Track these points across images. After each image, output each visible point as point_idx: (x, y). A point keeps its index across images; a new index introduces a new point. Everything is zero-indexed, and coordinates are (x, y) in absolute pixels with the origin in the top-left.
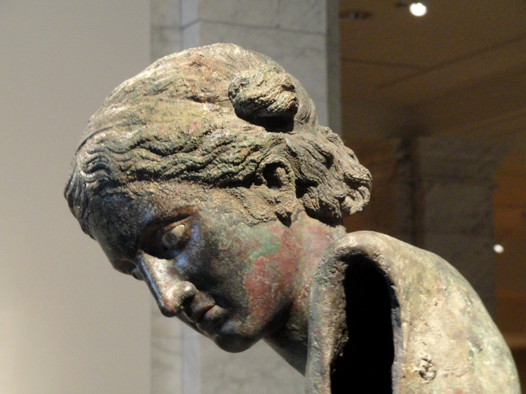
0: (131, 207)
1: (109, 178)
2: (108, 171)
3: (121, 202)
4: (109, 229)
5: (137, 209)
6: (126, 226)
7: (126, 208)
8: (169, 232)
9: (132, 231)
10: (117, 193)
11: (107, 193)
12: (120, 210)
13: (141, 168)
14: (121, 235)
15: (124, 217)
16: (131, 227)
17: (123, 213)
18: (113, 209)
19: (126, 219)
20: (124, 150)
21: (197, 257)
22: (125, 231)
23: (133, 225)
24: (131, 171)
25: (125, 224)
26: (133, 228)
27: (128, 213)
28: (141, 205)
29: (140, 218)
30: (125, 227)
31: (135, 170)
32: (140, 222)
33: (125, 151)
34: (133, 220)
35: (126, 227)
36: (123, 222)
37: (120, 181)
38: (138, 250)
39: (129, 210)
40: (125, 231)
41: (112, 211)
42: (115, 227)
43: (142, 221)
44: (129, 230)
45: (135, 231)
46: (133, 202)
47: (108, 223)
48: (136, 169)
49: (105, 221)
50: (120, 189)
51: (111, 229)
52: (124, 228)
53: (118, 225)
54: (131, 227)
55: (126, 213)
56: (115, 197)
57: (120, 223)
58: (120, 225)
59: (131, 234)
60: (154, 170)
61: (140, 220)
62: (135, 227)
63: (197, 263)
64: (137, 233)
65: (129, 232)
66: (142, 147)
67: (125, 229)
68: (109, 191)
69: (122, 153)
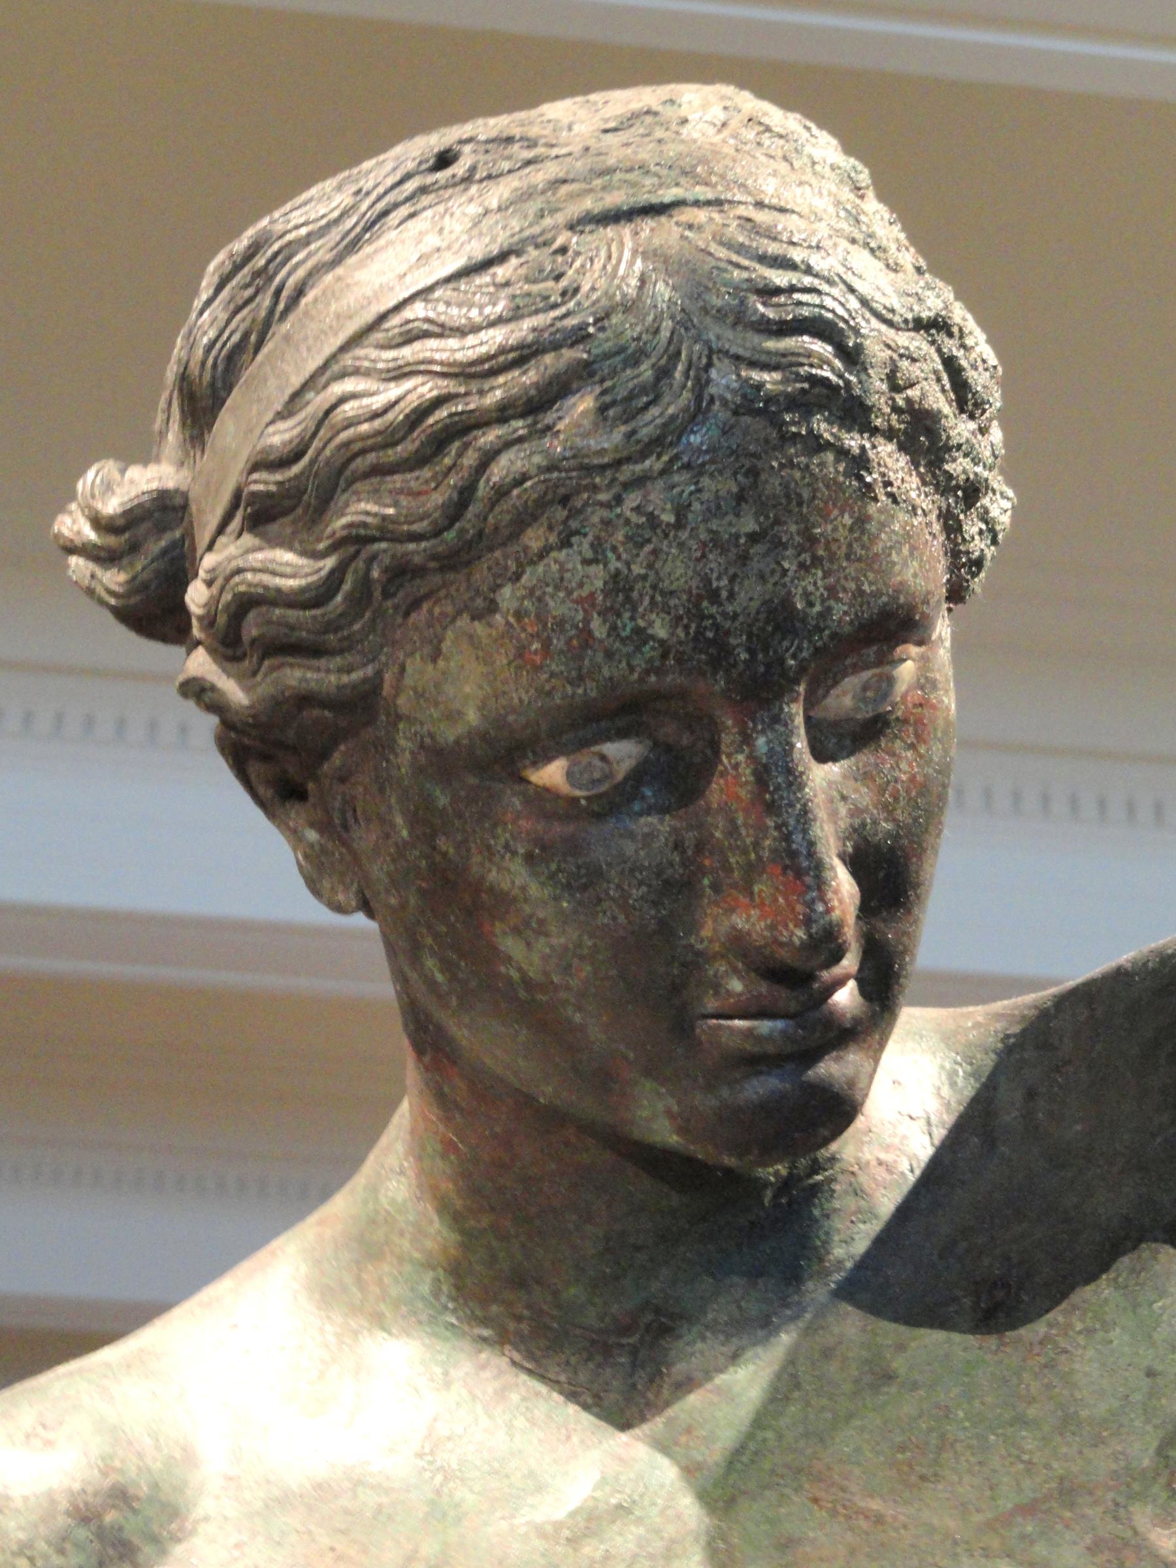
0: (862, 521)
1: (848, 383)
2: (852, 357)
3: (840, 485)
4: (744, 558)
5: (874, 539)
6: (820, 583)
7: (847, 520)
8: (887, 668)
9: (829, 609)
10: (842, 453)
11: (810, 431)
12: (825, 516)
13: (935, 406)
14: (786, 603)
15: (827, 548)
16: (832, 591)
17: (829, 527)
18: (806, 494)
19: (832, 558)
20: (897, 319)
21: (908, 791)
22: (806, 595)
23: (845, 590)
24: (908, 400)
25: (820, 573)
26: (838, 600)
27: (846, 538)
28: (886, 533)
29: (871, 576)
30: (815, 584)
31: (917, 406)
32: (866, 587)
33: (903, 326)
34: (851, 570)
35: (814, 584)
36: (817, 561)
37: (873, 416)
38: (799, 684)
39: (851, 530)
40: (806, 595)
41: (800, 504)
42: (778, 563)
43: (874, 588)
44: (823, 601)
45: (839, 610)
46: (872, 509)
47: (753, 538)
48: (920, 403)
49: (749, 525)
50: (853, 442)
51: (755, 565)
52: (807, 583)
53: (795, 563)
54: (832, 591)
55: (842, 534)
56: (830, 457)
57: (806, 557)
58: (802, 566)
59: (821, 615)
60: (949, 437)
61: (870, 584)
62: (846, 600)
63: (899, 815)
64: (840, 622)
65: (818, 608)
66: (933, 343)
67: (811, 588)
68: (823, 427)
69: (890, 323)
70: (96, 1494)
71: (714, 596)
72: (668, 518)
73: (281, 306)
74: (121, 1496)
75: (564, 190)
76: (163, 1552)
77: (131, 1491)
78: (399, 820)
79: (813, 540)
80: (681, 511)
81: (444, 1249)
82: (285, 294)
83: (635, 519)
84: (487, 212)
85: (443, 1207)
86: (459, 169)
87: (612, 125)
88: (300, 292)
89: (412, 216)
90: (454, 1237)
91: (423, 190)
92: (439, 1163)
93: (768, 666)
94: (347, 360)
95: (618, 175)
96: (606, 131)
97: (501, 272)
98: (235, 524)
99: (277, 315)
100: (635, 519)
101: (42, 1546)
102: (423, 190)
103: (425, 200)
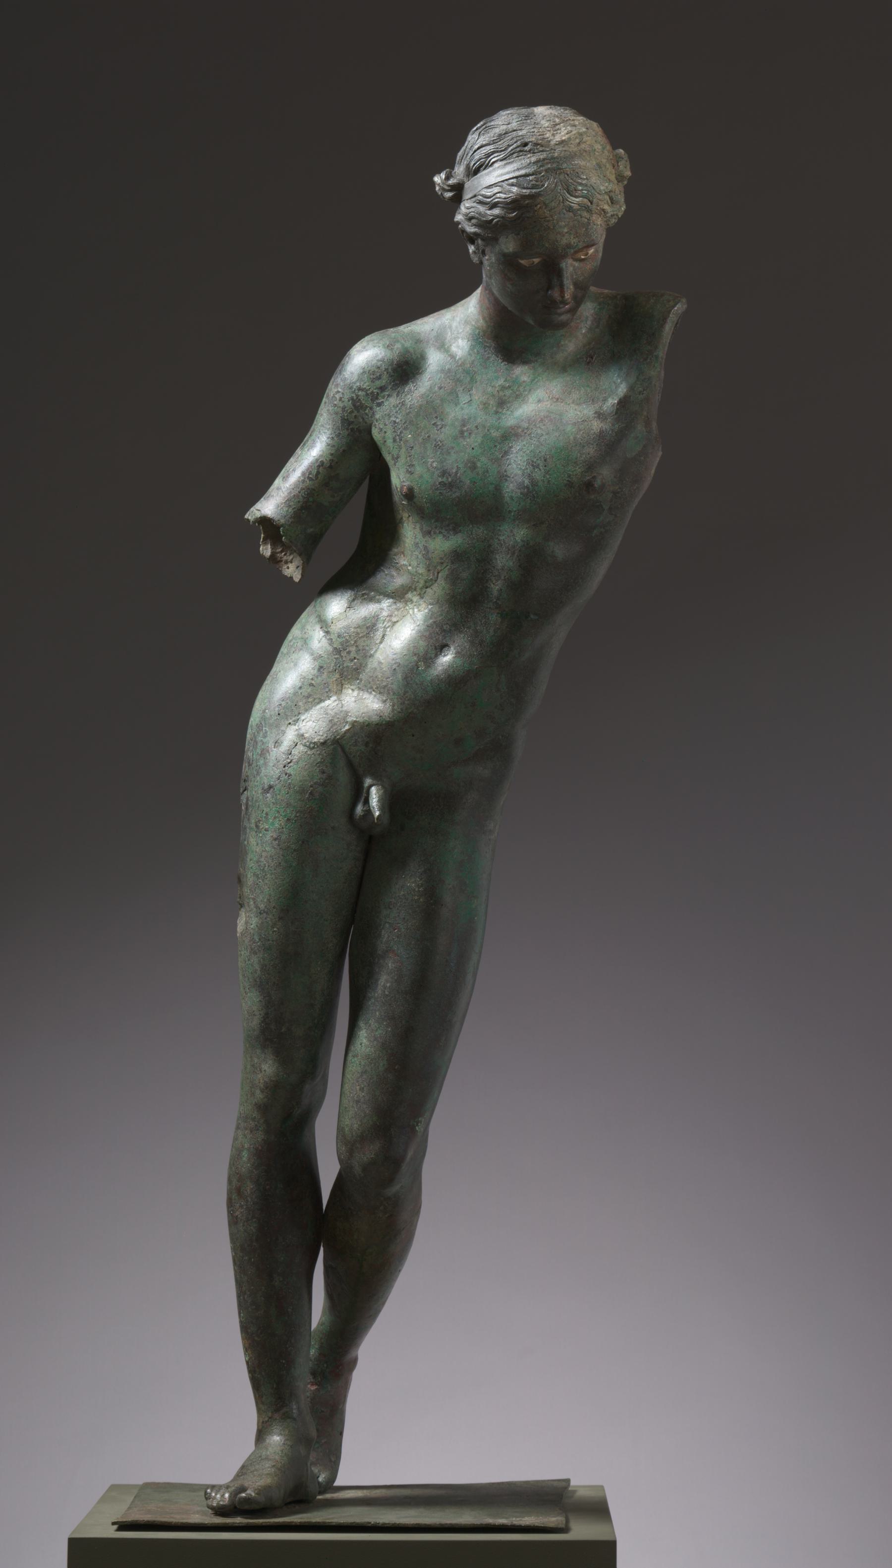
7: (584, 229)
54: (579, 242)
57: (575, 236)
70: (402, 362)
71: (557, 241)
72: (552, 228)
73: (490, 164)
74: (407, 363)
75: (546, 161)
76: (414, 376)
77: (409, 362)
78: (493, 258)
79: (577, 233)
80: (554, 227)
81: (482, 327)
82: (491, 162)
83: (546, 227)
84: (530, 163)
85: (484, 318)
86: (526, 148)
87: (557, 143)
88: (494, 162)
89: (518, 157)
90: (485, 325)
91: (521, 151)
92: (485, 311)
93: (565, 253)
94: (500, 184)
95: (556, 160)
96: (557, 144)
97: (531, 178)
98: (474, 199)
99: (490, 164)
100: (546, 227)
101: (390, 370)
102: (521, 151)
103: (521, 154)
